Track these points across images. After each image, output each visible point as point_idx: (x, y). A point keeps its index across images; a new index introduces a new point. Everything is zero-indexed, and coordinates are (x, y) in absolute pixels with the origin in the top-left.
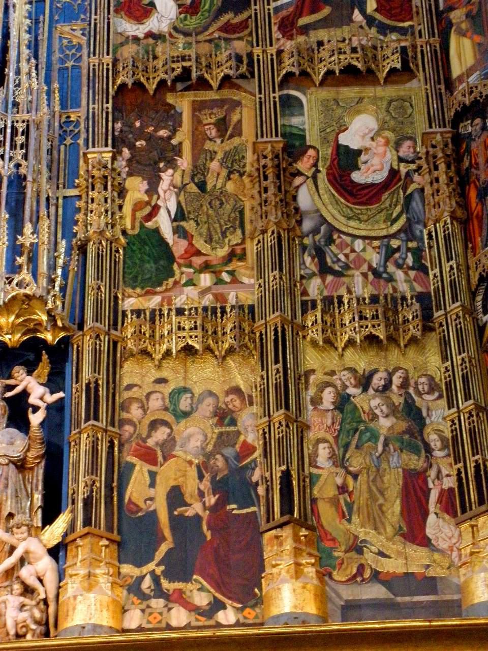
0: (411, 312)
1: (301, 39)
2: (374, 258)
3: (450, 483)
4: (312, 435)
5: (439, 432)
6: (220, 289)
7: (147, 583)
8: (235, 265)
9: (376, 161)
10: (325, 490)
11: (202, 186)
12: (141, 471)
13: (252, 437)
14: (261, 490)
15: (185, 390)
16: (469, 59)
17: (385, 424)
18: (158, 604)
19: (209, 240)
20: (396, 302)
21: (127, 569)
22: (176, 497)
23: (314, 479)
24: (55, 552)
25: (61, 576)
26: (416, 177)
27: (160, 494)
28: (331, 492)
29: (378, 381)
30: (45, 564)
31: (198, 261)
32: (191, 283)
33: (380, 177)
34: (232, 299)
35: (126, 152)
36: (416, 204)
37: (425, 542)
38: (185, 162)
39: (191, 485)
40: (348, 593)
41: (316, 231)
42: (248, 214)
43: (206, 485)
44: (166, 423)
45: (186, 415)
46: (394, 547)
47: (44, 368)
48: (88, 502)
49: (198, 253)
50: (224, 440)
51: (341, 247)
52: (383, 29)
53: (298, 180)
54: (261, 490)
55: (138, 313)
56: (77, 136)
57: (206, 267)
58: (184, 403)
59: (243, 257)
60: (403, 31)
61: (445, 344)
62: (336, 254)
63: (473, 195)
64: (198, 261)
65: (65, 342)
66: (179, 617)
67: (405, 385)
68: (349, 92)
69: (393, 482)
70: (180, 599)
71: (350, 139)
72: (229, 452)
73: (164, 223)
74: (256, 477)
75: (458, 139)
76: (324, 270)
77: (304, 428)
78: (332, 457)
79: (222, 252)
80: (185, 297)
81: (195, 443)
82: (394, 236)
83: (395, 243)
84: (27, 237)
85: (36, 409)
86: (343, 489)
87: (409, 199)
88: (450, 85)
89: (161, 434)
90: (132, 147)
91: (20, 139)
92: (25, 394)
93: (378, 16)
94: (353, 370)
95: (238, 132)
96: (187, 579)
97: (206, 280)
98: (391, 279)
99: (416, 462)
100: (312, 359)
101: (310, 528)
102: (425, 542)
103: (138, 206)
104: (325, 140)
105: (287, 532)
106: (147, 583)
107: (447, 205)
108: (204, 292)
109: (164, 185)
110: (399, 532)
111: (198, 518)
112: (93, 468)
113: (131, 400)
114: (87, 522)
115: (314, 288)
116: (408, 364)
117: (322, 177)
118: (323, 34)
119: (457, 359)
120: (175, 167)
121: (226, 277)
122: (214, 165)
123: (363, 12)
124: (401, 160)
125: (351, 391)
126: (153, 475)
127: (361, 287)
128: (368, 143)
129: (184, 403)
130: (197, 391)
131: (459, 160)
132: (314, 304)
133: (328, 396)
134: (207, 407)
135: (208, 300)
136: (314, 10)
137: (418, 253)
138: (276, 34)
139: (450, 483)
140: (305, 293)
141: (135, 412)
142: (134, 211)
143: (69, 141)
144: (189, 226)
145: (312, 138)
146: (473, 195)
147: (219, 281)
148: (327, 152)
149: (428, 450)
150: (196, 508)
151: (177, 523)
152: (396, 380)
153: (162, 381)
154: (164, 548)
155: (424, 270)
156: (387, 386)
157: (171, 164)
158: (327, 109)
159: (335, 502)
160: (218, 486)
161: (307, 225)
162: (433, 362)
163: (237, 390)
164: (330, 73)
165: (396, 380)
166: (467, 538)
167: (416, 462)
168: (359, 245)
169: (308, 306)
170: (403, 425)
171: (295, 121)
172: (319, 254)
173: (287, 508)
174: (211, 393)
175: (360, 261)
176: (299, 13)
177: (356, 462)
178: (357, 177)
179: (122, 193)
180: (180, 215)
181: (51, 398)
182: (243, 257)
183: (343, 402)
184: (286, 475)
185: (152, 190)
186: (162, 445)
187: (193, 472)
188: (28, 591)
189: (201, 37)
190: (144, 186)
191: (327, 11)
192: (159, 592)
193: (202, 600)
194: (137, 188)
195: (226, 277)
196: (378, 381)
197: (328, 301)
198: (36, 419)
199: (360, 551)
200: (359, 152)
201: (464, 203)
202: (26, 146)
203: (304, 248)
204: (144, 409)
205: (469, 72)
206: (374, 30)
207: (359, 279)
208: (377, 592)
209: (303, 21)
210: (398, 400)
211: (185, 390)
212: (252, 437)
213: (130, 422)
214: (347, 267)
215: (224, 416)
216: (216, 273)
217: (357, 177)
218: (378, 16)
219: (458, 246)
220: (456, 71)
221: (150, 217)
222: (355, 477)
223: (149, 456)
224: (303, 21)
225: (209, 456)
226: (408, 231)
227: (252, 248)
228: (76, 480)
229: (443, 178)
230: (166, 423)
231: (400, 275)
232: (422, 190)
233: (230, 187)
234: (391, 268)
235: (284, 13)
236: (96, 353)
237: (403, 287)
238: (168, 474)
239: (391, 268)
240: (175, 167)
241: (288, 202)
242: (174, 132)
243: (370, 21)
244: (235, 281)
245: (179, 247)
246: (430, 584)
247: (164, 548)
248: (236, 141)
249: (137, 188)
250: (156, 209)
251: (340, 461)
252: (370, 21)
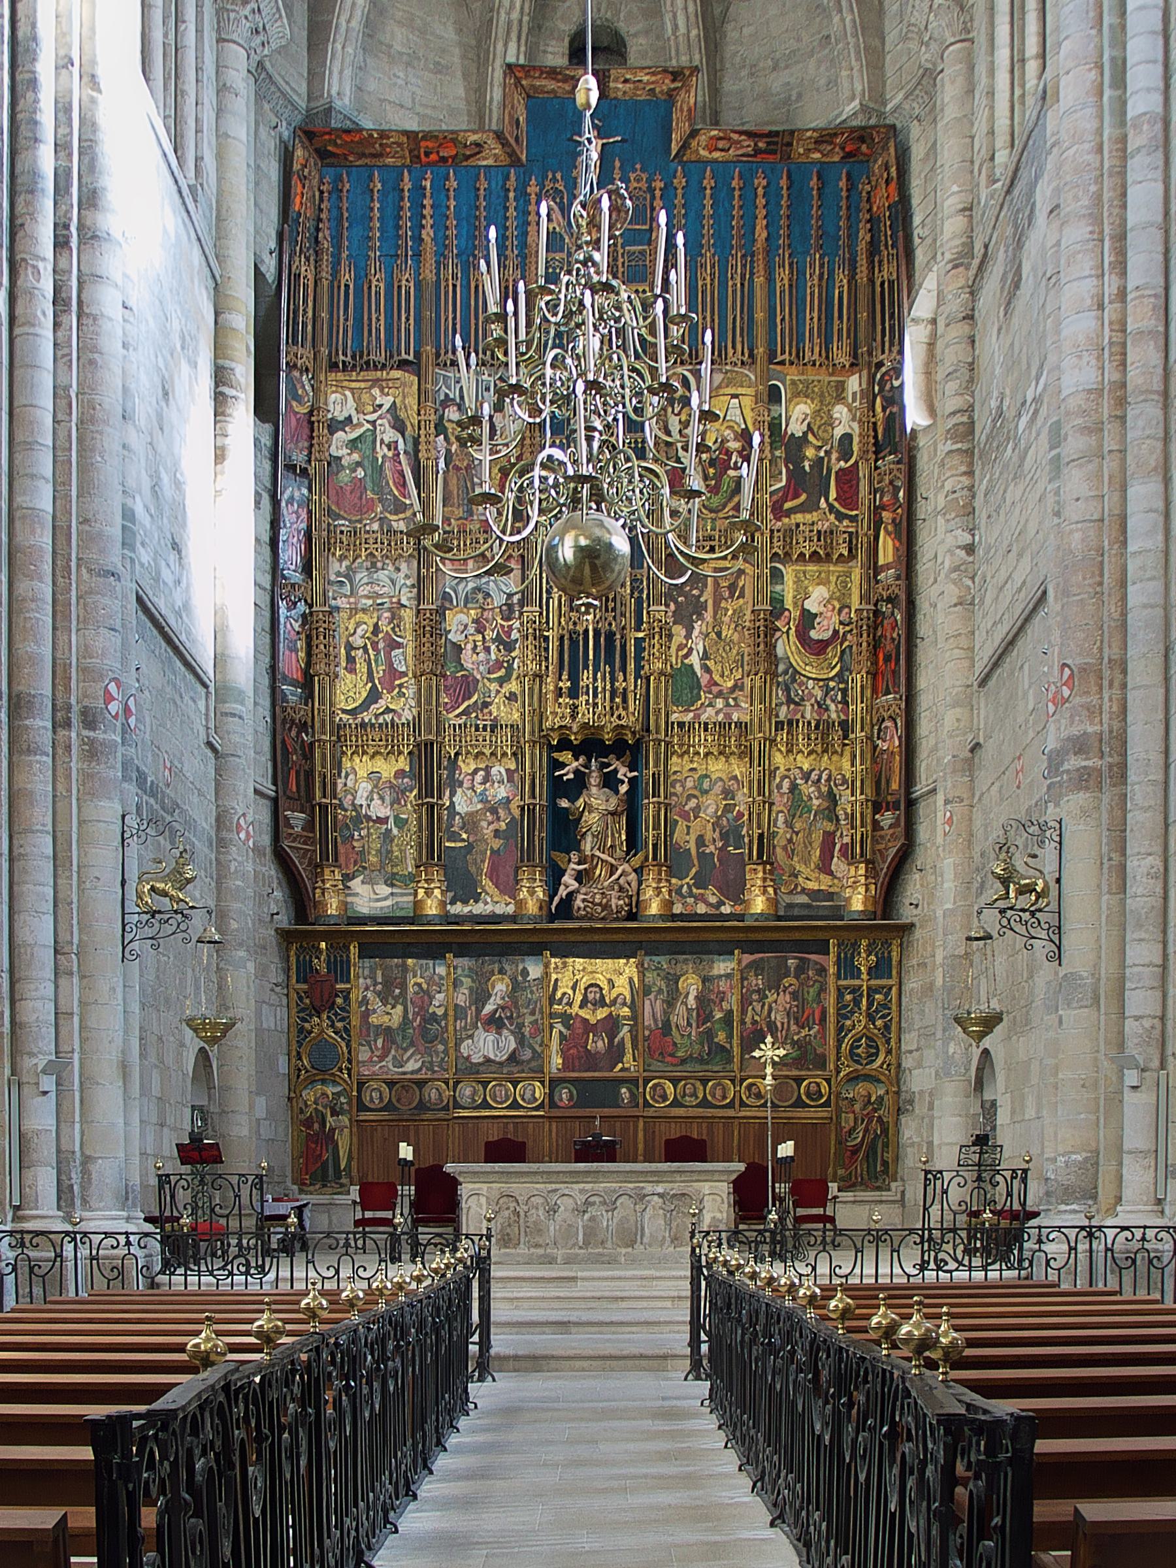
0: (836, 736)
1: (786, 520)
2: (819, 694)
3: (847, 840)
4: (774, 808)
5: (844, 809)
6: (728, 710)
7: (685, 888)
8: (737, 693)
9: (825, 623)
10: (780, 841)
11: (719, 634)
12: (682, 825)
13: (742, 808)
14: (746, 840)
15: (706, 776)
16: (890, 559)
17: (816, 802)
18: (690, 900)
19: (722, 676)
20: (829, 725)
21: (674, 881)
22: (701, 842)
23: (773, 835)
24: (635, 871)
25: (640, 883)
26: (849, 636)
27: (692, 838)
28: (784, 842)
29: (814, 776)
30: (633, 877)
31: (715, 689)
32: (710, 705)
33: (826, 635)
34: (735, 717)
35: (672, 606)
36: (847, 657)
37: (831, 873)
38: (708, 615)
39: (709, 836)
40: (788, 899)
41: (786, 672)
42: (746, 658)
43: (717, 835)
44: (695, 797)
45: (706, 792)
46: (813, 876)
47: (628, 757)
48: (655, 846)
49: (716, 684)
50: (728, 809)
51: (800, 685)
52: (840, 517)
53: (778, 634)
54: (746, 840)
55: (681, 725)
56: (641, 592)
57: (720, 694)
58: (706, 786)
59: (742, 689)
60: (853, 519)
61: (854, 757)
62: (797, 691)
63: (881, 656)
64: (715, 689)
65: (638, 743)
66: (701, 909)
67: (829, 780)
68: (811, 568)
69: (817, 837)
70: (701, 898)
71: (812, 605)
72: (730, 816)
73: (694, 660)
74: (744, 832)
75: (876, 613)
76: (790, 701)
77: (771, 804)
78: (786, 822)
79: (730, 684)
80: (708, 714)
81: (711, 810)
82: (832, 679)
83: (832, 684)
84: (620, 685)
85: (623, 782)
86: (790, 841)
87: (843, 652)
88: (877, 570)
89: (693, 803)
90: (676, 602)
91: (611, 605)
92: (616, 771)
93: (836, 505)
94: (801, 768)
95: (742, 595)
96: (706, 888)
97: (720, 703)
98: (827, 709)
99: (830, 827)
100: (778, 759)
101: (772, 864)
102: (831, 873)
103: (680, 647)
104: (795, 604)
105: (760, 868)
106: (685, 888)
107: (866, 665)
108: (717, 713)
109: (696, 633)
110: (817, 867)
111: (712, 854)
112: (656, 827)
113: (676, 781)
114: (655, 858)
115: (783, 712)
116: (832, 768)
117: (792, 632)
118: (799, 518)
119: (859, 768)
120: (703, 620)
121: (732, 702)
122: (726, 619)
123: (827, 500)
124: (841, 623)
125: (799, 781)
126: (688, 827)
127: (809, 713)
128: (822, 609)
129: (706, 786)
130: (714, 777)
131: (876, 629)
132: (782, 723)
133: (786, 784)
134: (718, 788)
135: (720, 717)
136: (796, 496)
137: (844, 692)
138: (770, 516)
139: (847, 840)
140: (777, 716)
141: (679, 789)
142: (678, 650)
143: (636, 594)
144: (710, 664)
145: (789, 604)
146: (881, 656)
147: (728, 705)
148: (796, 614)
149: (838, 820)
150: (712, 848)
151: (702, 856)
152: (824, 776)
153: (692, 770)
154: (694, 871)
155: (847, 704)
156: (819, 780)
157: (700, 617)
158: (798, 581)
159: (785, 848)
160: (724, 836)
161: (781, 668)
162: (846, 764)
163: (735, 778)
164: (802, 555)
165: (824, 776)
166: (852, 873)
167: (830, 827)
168: (811, 683)
169: (779, 726)
170: (826, 804)
171: (778, 588)
172: (787, 690)
173: (760, 855)
174: (721, 779)
175: (811, 695)
176: (785, 499)
177: (798, 826)
178: (813, 634)
179: (670, 636)
180: (705, 656)
181: (630, 775)
182: (742, 689)
183: (794, 787)
184: (761, 836)
185: (688, 636)
186: (693, 810)
187: (710, 826)
188: (621, 889)
189: (721, 515)
190: (683, 632)
191: (804, 497)
192: (691, 895)
193: (713, 900)
194: (679, 631)
195: (732, 702)
196: (814, 776)
197: (790, 723)
198: (624, 788)
199: (796, 876)
200: (816, 615)
201: (875, 663)
202: (614, 610)
203: (778, 684)
204: (683, 786)
205: (888, 567)
206: (832, 517)
207: (809, 708)
208: (803, 899)
209: (787, 505)
210: (824, 789)
211: (706, 776)
212: (742, 808)
213: (675, 794)
214: (803, 699)
215: (728, 793)
216: (727, 699)
217: (813, 634)
218: (836, 505)
219: (868, 693)
220: (881, 562)
221: (686, 656)
222: (797, 833)
223: (685, 816)
224: (787, 505)
225: (719, 818)
226: (840, 677)
227: (747, 682)
228: (647, 830)
229: (864, 644)
230: (695, 797)
231: (833, 707)
232: (850, 647)
233: (736, 637)
234: (828, 702)
235: (775, 498)
236: (657, 754)
237: (834, 716)
238: (696, 825)
239: (828, 702)
240: (703, 620)
241: (771, 647)
242: (702, 592)
243: (831, 507)
244: (737, 705)
245: (704, 679)
246: (830, 896)
247: (694, 871)
248: (741, 601)
249: (679, 631)
250: (691, 649)
251: (789, 825)
252: (831, 507)
